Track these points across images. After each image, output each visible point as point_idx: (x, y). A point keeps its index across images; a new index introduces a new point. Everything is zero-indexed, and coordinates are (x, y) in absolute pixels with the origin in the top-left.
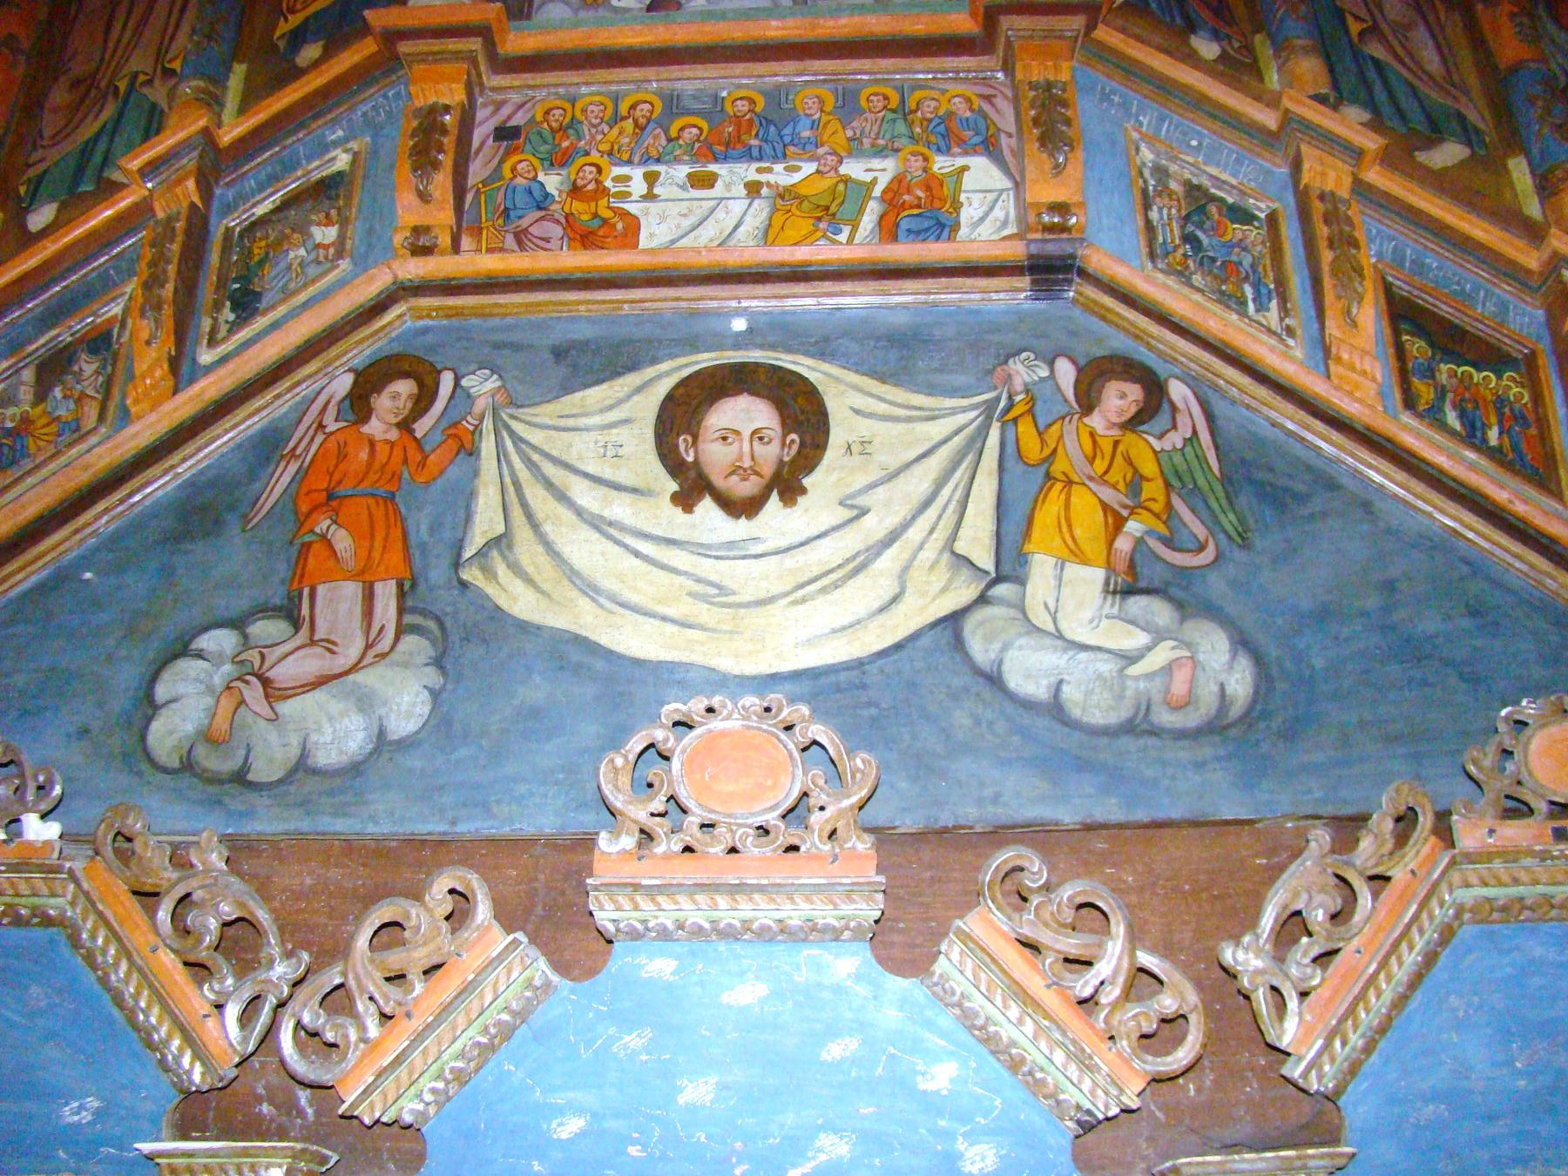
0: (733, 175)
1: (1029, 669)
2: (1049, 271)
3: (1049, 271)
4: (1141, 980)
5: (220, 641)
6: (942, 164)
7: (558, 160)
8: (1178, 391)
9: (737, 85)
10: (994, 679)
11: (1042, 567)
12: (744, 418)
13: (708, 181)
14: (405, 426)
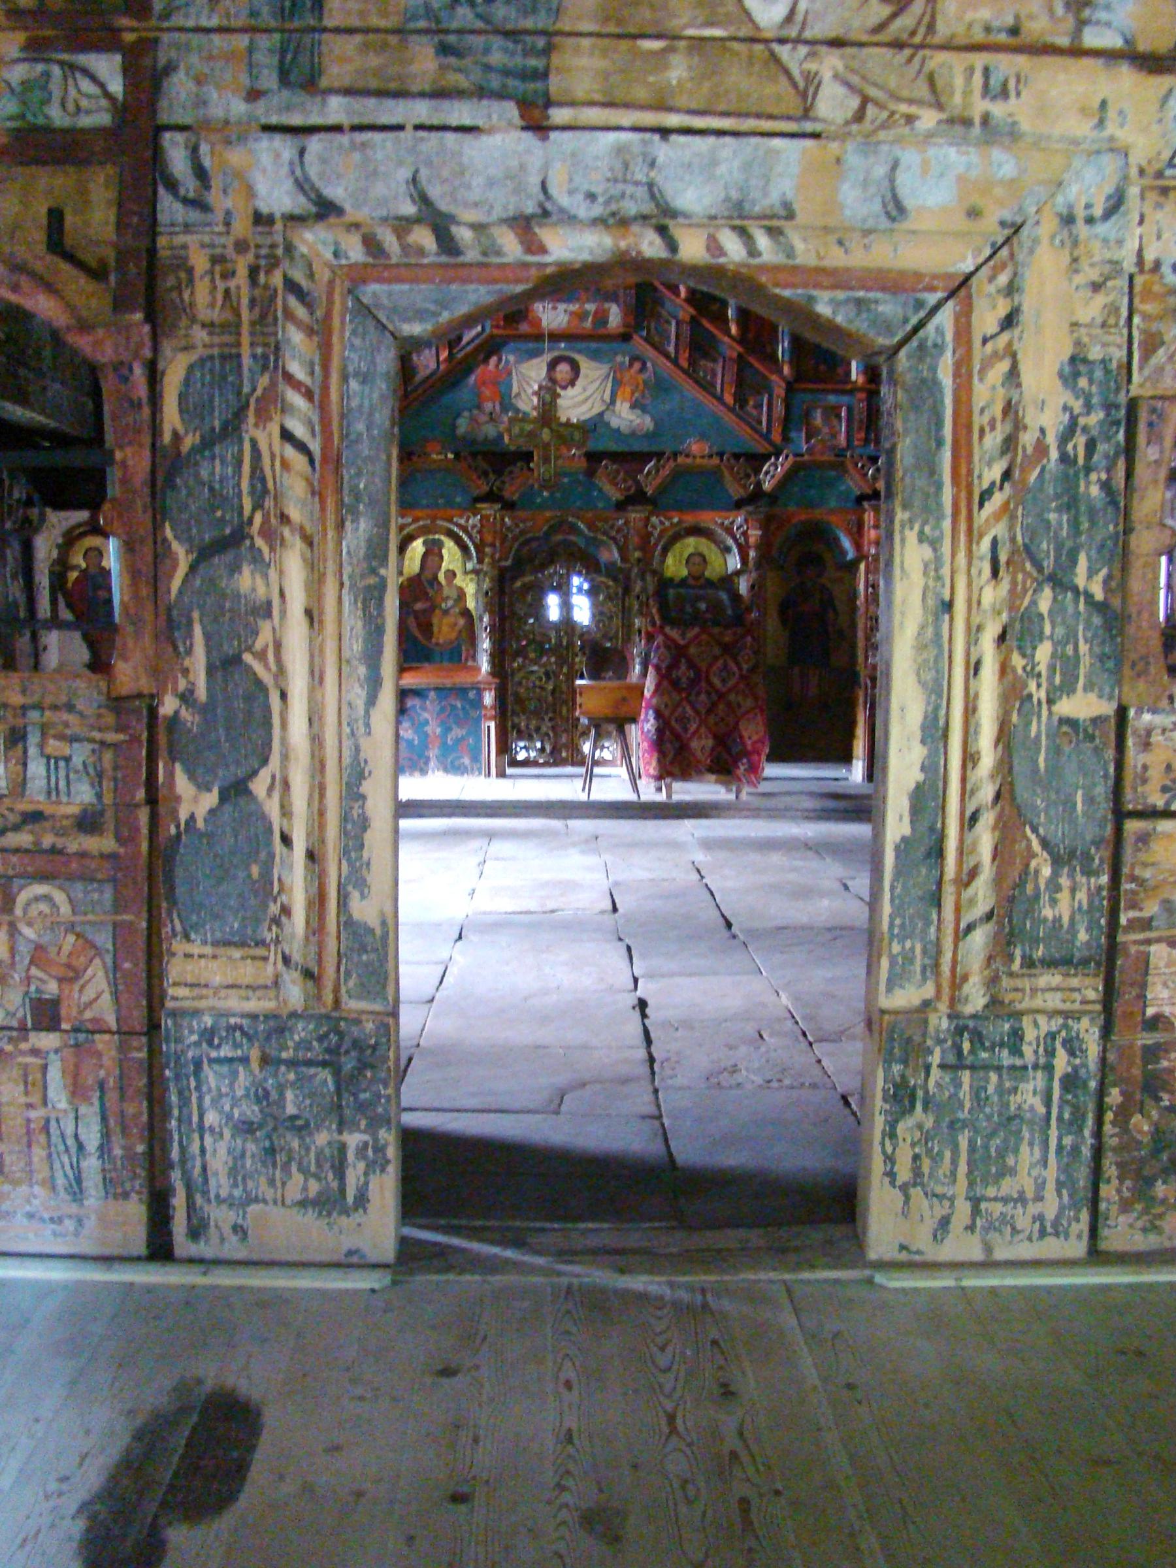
0: (562, 307)
1: (615, 423)
4: (625, 481)
6: (606, 305)
8: (649, 365)
10: (608, 424)
11: (618, 403)
12: (563, 369)
13: (555, 308)
14: (497, 366)
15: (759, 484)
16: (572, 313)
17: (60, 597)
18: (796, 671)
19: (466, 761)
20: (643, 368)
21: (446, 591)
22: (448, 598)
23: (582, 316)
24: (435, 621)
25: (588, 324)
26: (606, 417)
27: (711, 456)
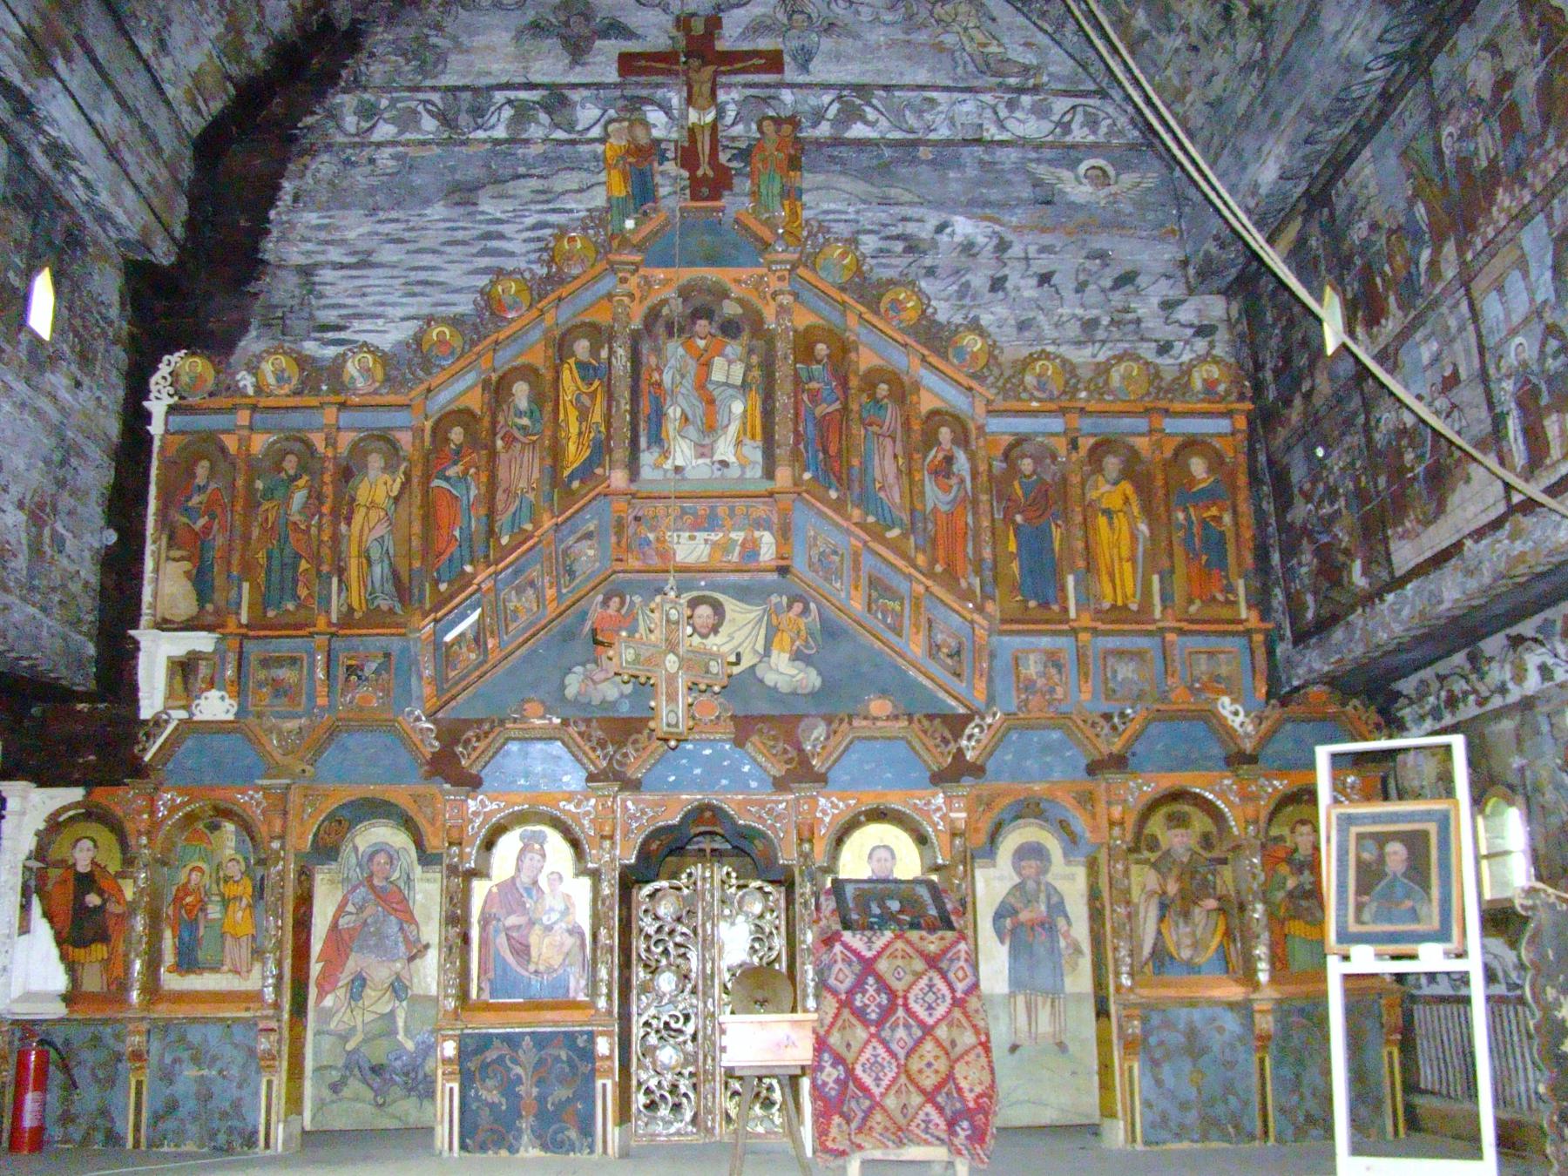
0: (701, 536)
1: (770, 679)
2: (783, 571)
3: (783, 571)
4: (785, 751)
5: (578, 669)
7: (653, 529)
8: (812, 606)
9: (702, 507)
10: (761, 681)
11: (775, 653)
12: (704, 611)
13: (692, 538)
15: (960, 753)
16: (715, 544)
17: (35, 901)
18: (1021, 999)
19: (573, 1134)
20: (805, 611)
21: (549, 901)
22: (552, 909)
23: (724, 547)
24: (533, 940)
25: (735, 557)
26: (759, 672)
27: (896, 717)
